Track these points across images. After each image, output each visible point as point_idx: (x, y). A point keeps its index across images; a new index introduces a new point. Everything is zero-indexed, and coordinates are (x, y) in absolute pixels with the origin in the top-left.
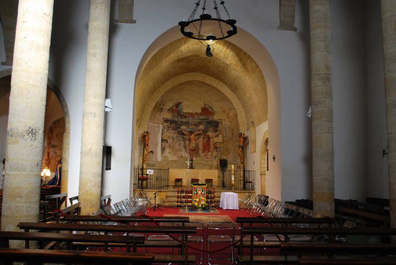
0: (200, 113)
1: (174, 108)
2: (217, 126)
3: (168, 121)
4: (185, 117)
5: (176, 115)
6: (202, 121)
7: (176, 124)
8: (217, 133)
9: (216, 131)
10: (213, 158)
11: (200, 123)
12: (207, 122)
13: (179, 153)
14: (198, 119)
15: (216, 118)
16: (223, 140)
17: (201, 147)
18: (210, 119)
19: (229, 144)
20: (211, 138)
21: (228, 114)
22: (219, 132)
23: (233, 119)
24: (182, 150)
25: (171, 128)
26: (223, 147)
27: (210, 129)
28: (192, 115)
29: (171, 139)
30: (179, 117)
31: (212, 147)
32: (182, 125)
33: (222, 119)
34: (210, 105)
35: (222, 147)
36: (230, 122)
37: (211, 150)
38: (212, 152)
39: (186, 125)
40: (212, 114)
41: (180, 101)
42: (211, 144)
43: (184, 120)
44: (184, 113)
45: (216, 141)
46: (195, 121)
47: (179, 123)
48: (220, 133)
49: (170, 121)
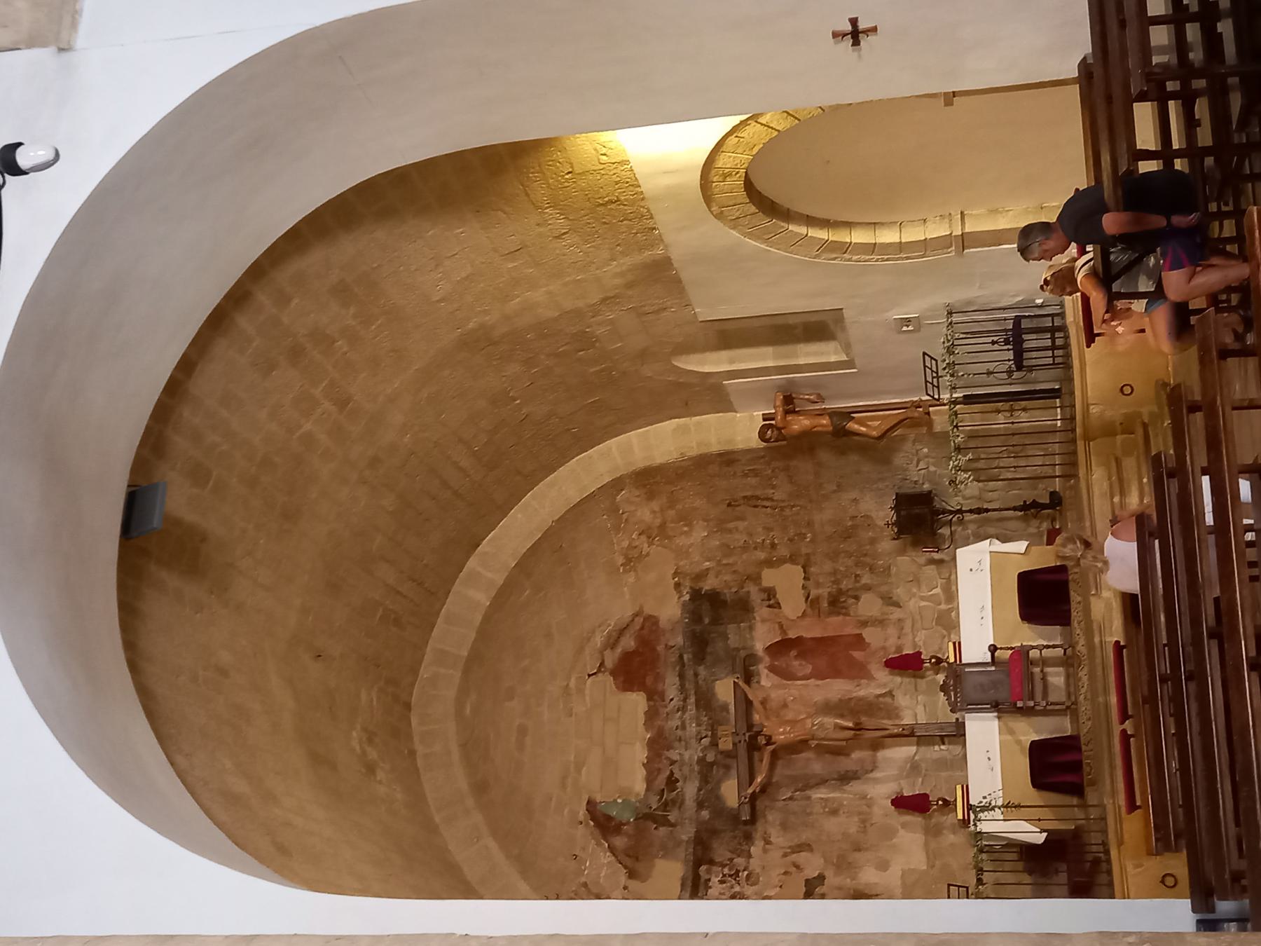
0: (649, 699)
1: (620, 842)
2: (714, 599)
3: (696, 877)
4: (672, 782)
5: (663, 830)
6: (690, 686)
7: (714, 833)
8: (756, 597)
9: (743, 608)
10: (896, 614)
11: (705, 701)
12: (700, 657)
13: (876, 810)
14: (683, 709)
15: (670, 610)
16: (792, 559)
17: (838, 688)
18: (679, 640)
19: (810, 524)
20: (783, 631)
21: (646, 532)
22: (752, 589)
23: (672, 503)
24: (864, 797)
25: (739, 861)
26: (834, 556)
27: (733, 641)
28: (658, 745)
29: (802, 857)
30: (673, 816)
31: (834, 626)
32: (718, 798)
33: (676, 574)
34: (598, 640)
35: (828, 566)
36: (686, 519)
37: (850, 630)
38: (864, 624)
39: (719, 782)
40: (648, 629)
41: (582, 813)
42: (817, 633)
43: (690, 790)
44: (648, 790)
45: (803, 606)
46: (692, 729)
47: (705, 814)
48: (756, 579)
49: (697, 864)
